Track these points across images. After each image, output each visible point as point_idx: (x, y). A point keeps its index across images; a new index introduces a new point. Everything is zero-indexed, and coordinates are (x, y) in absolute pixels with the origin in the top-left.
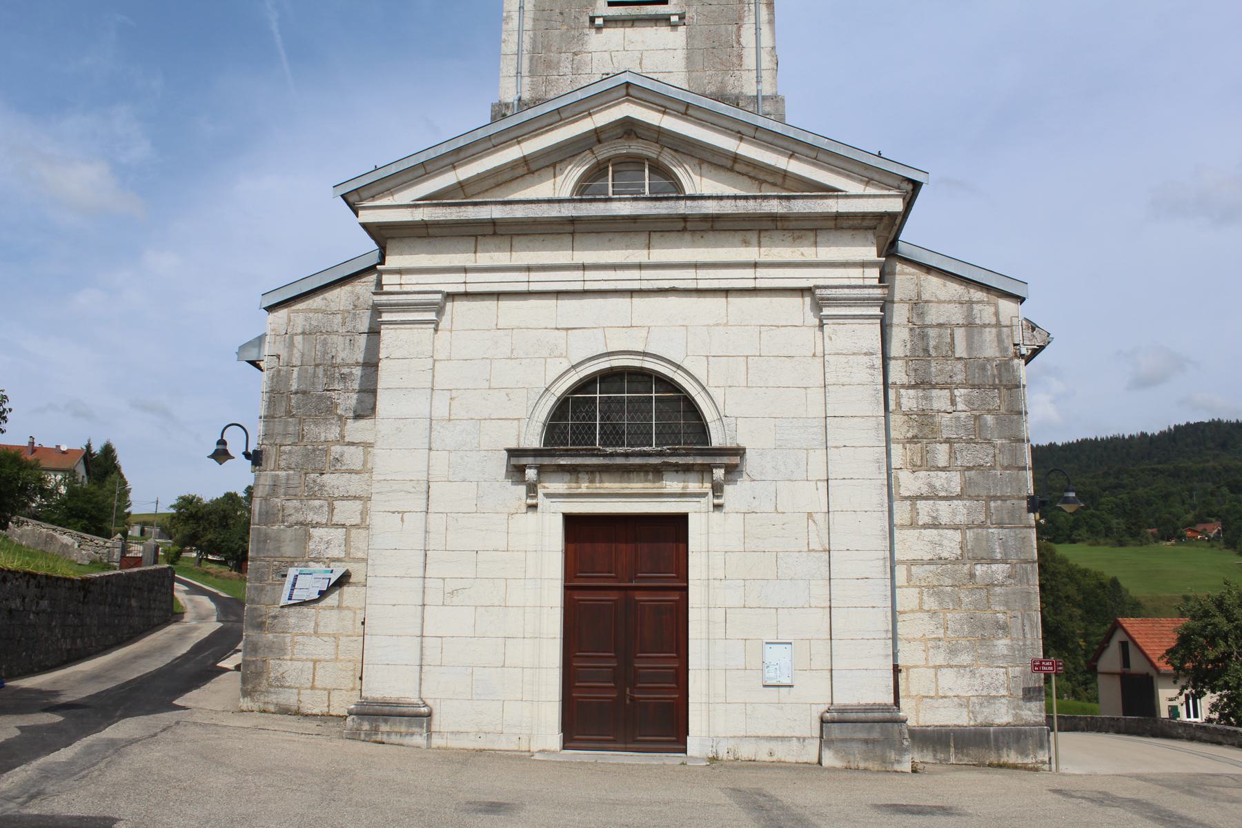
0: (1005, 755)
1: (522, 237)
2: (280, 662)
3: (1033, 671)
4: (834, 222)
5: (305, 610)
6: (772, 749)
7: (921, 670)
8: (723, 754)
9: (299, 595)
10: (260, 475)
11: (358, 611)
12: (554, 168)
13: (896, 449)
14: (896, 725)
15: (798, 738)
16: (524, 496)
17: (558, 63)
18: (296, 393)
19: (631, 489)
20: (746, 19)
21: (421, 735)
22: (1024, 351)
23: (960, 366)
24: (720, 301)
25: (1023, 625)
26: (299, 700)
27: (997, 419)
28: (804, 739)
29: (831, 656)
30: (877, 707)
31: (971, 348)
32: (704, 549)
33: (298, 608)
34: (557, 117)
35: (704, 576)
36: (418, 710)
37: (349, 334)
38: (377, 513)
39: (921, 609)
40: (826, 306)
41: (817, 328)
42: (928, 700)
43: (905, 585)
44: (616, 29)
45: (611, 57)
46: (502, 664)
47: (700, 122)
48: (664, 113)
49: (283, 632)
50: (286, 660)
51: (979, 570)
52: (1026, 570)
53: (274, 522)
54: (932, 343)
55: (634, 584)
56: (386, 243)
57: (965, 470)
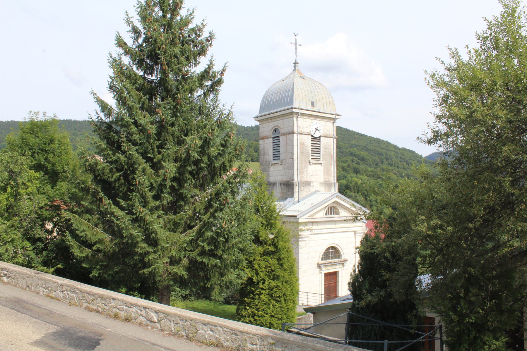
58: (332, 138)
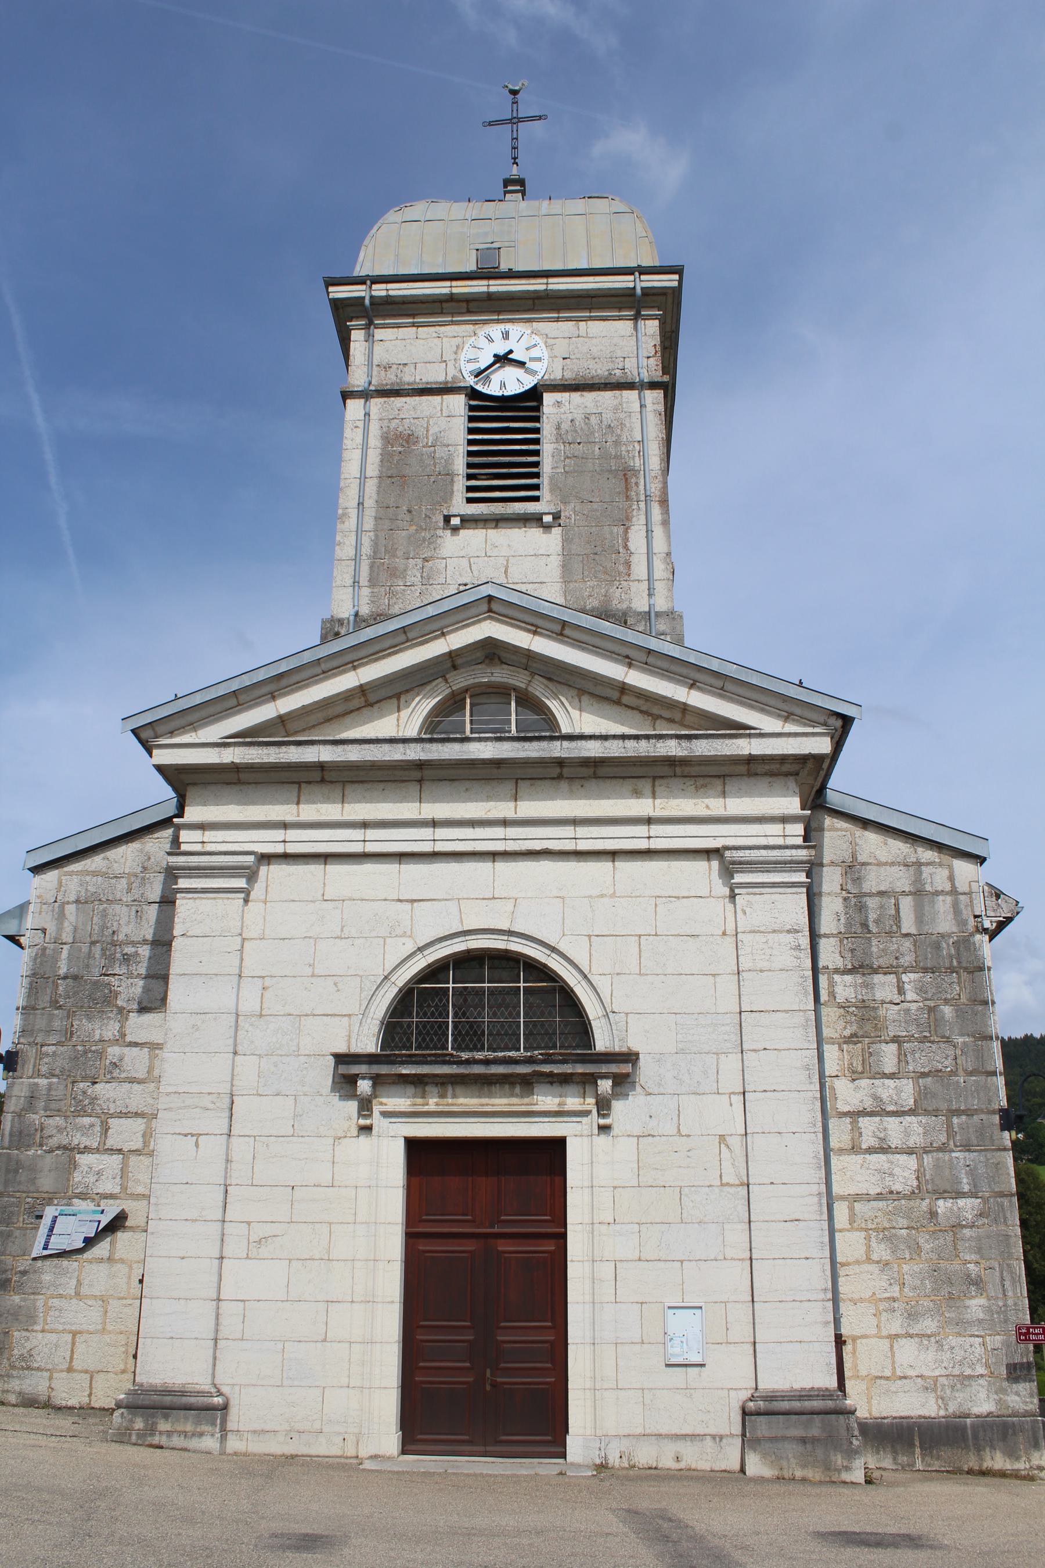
0: (988, 1458)
1: (356, 785)
2: (28, 1334)
3: (1019, 1341)
4: (747, 767)
5: (65, 1263)
6: (678, 1452)
7: (873, 1341)
8: (614, 1460)
9: (58, 1243)
10: (13, 1084)
11: (135, 1266)
12: (399, 699)
13: (831, 1052)
14: (841, 1416)
15: (714, 1437)
16: (356, 1115)
17: (405, 570)
18: (65, 978)
19: (493, 1105)
20: (634, 519)
21: (212, 1435)
22: (987, 924)
23: (907, 944)
24: (604, 867)
25: (1002, 1279)
26: (50, 1387)
27: (957, 1011)
28: (721, 1437)
29: (754, 1324)
30: (816, 1393)
31: (922, 922)
32: (587, 1183)
33: (55, 1261)
34: (403, 638)
35: (587, 1220)
36: (209, 1400)
37: (136, 903)
38: (165, 1136)
39: (869, 1260)
40: (738, 872)
41: (727, 900)
42: (883, 1382)
43: (846, 1227)
44: (476, 531)
45: (470, 565)
46: (323, 1337)
47: (579, 644)
48: (535, 633)
49: (33, 1294)
50: (36, 1331)
51: (943, 1206)
52: (1001, 1206)
53: (28, 1146)
54: (872, 916)
55: (496, 1230)
56: (186, 790)
57: (919, 1077)
58: (630, 386)
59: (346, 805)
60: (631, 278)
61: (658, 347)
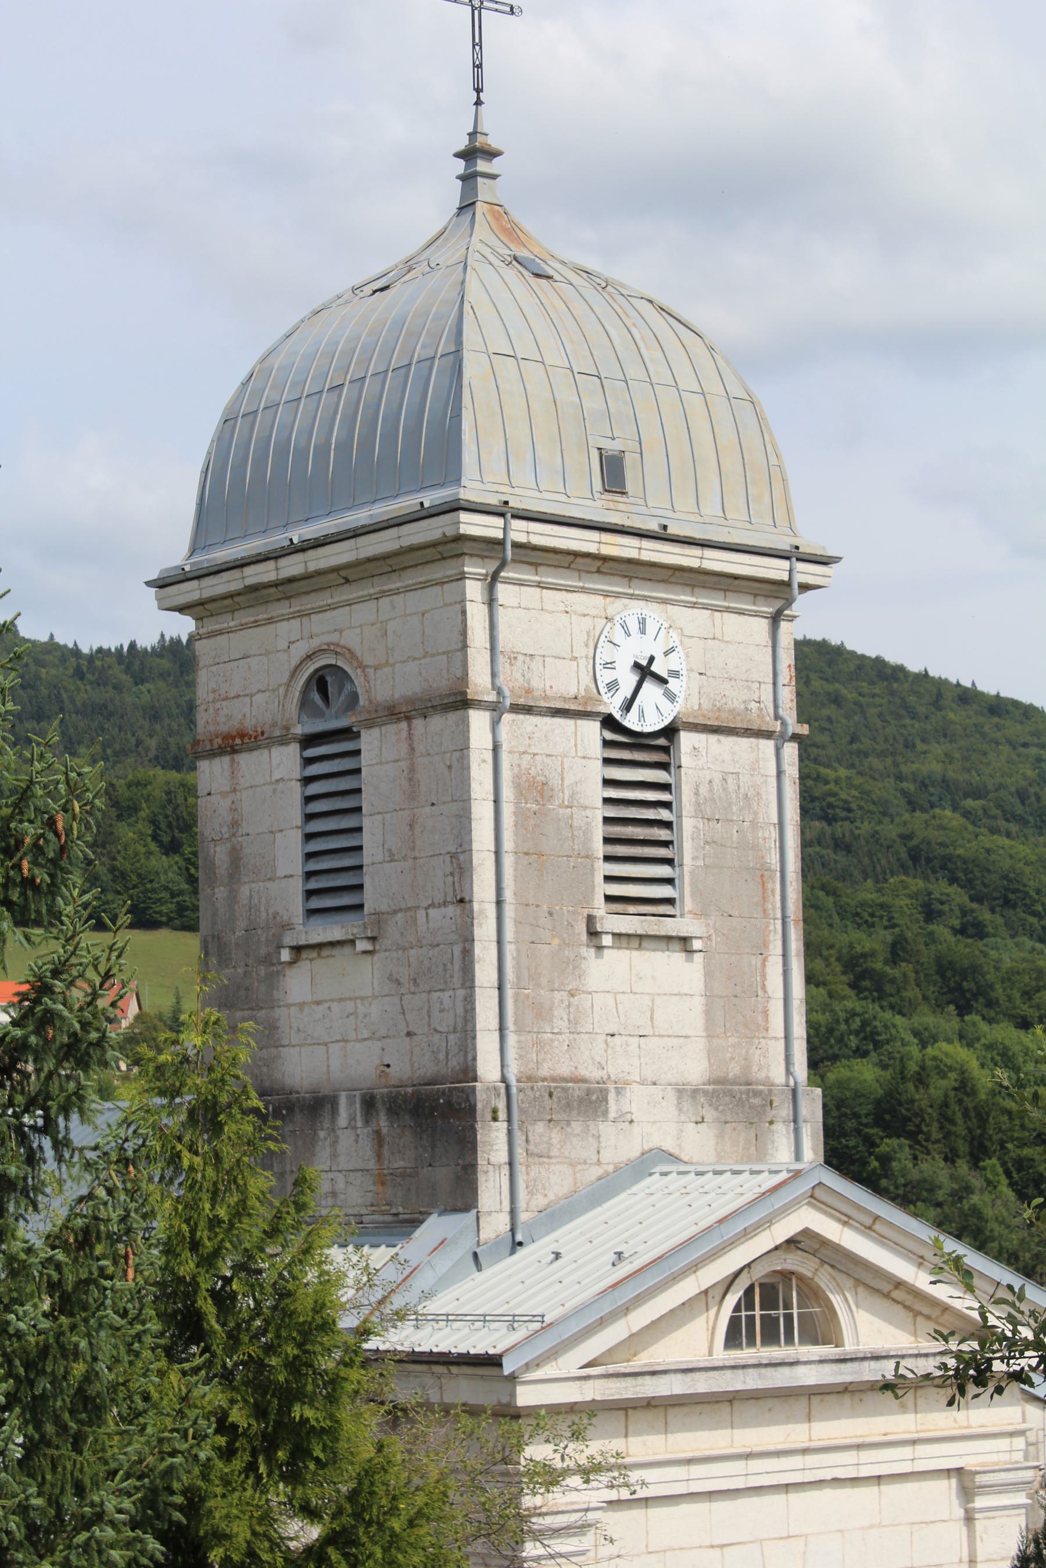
17: (551, 1009)
48: (845, 1224)
58: (768, 735)
59: (669, 1435)
60: (785, 564)
61: (793, 669)
